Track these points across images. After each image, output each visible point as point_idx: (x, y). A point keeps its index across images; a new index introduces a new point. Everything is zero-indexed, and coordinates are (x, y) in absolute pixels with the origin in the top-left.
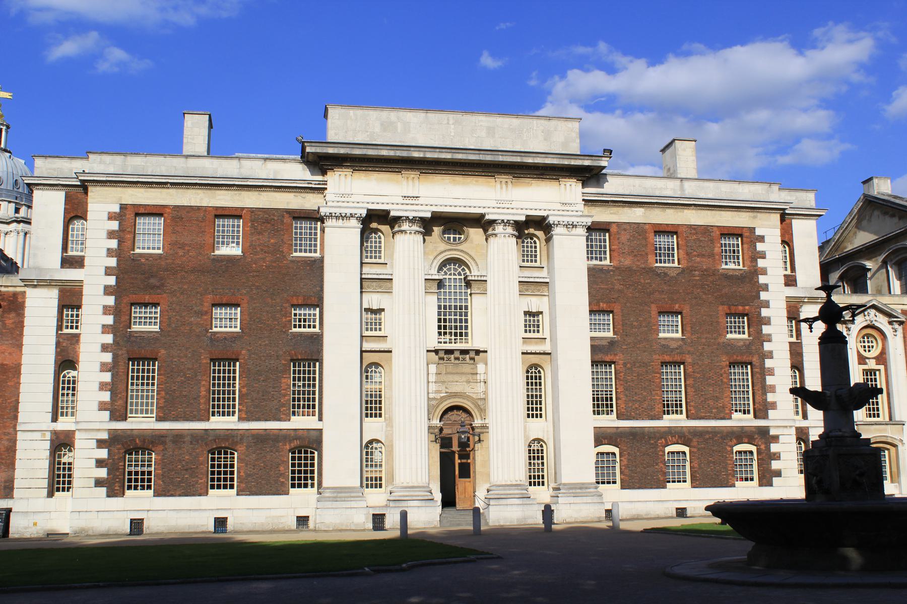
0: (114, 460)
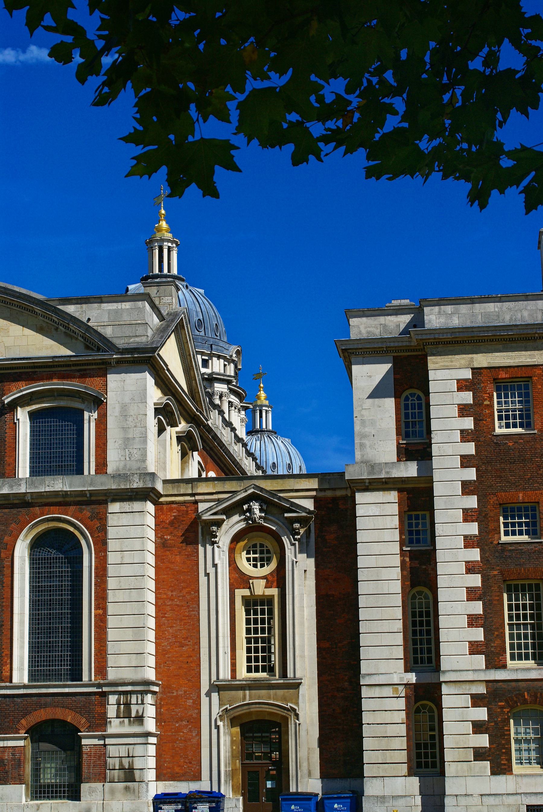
0: (496, 723)
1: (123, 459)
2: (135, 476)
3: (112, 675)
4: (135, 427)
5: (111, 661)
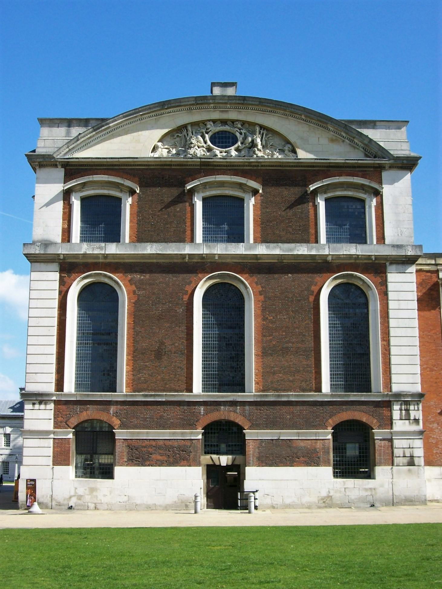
1: (396, 235)
2: (409, 246)
3: (395, 388)
4: (404, 212)
5: (394, 378)
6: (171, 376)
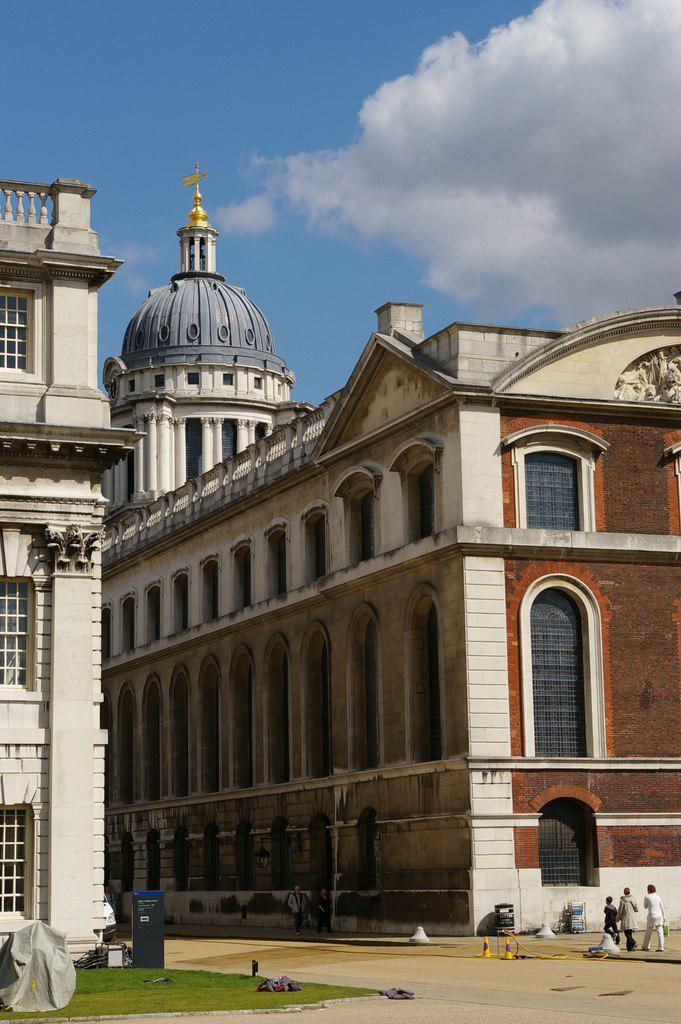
6: (663, 732)
